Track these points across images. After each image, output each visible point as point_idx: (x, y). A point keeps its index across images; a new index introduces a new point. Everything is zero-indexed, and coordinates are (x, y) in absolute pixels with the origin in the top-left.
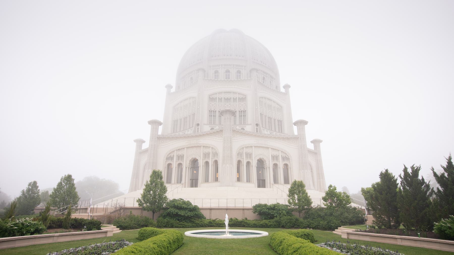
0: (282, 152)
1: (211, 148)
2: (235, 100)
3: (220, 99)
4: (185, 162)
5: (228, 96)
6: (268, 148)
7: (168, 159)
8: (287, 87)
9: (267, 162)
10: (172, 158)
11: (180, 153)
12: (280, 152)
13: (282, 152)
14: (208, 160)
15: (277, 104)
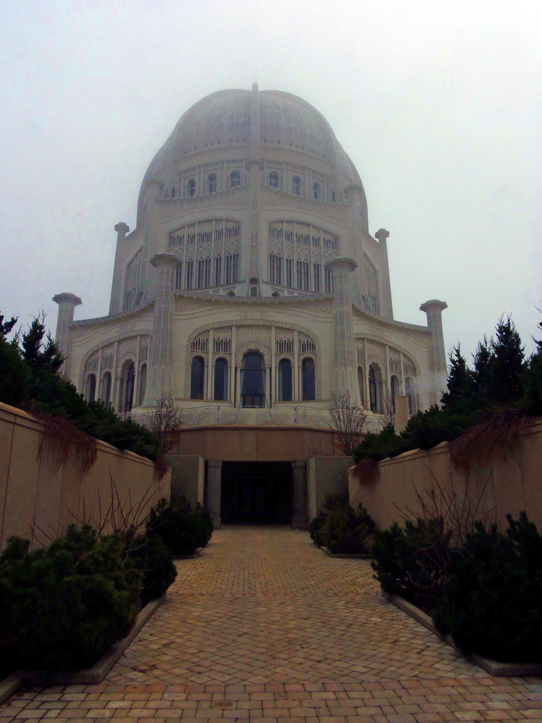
0: (404, 355)
1: (296, 333)
2: (316, 241)
3: (289, 236)
4: (233, 356)
5: (303, 231)
6: (383, 345)
7: (194, 345)
8: (383, 234)
9: (383, 372)
10: (203, 346)
11: (223, 336)
12: (402, 355)
13: (404, 355)
14: (290, 357)
15: (372, 265)
